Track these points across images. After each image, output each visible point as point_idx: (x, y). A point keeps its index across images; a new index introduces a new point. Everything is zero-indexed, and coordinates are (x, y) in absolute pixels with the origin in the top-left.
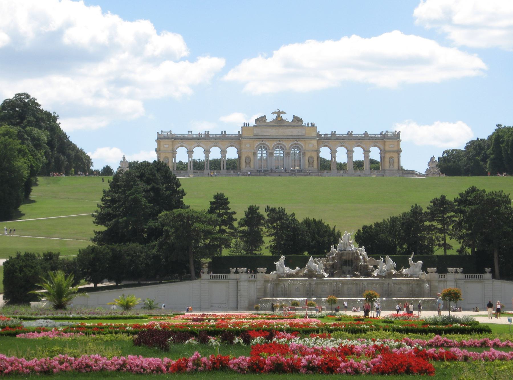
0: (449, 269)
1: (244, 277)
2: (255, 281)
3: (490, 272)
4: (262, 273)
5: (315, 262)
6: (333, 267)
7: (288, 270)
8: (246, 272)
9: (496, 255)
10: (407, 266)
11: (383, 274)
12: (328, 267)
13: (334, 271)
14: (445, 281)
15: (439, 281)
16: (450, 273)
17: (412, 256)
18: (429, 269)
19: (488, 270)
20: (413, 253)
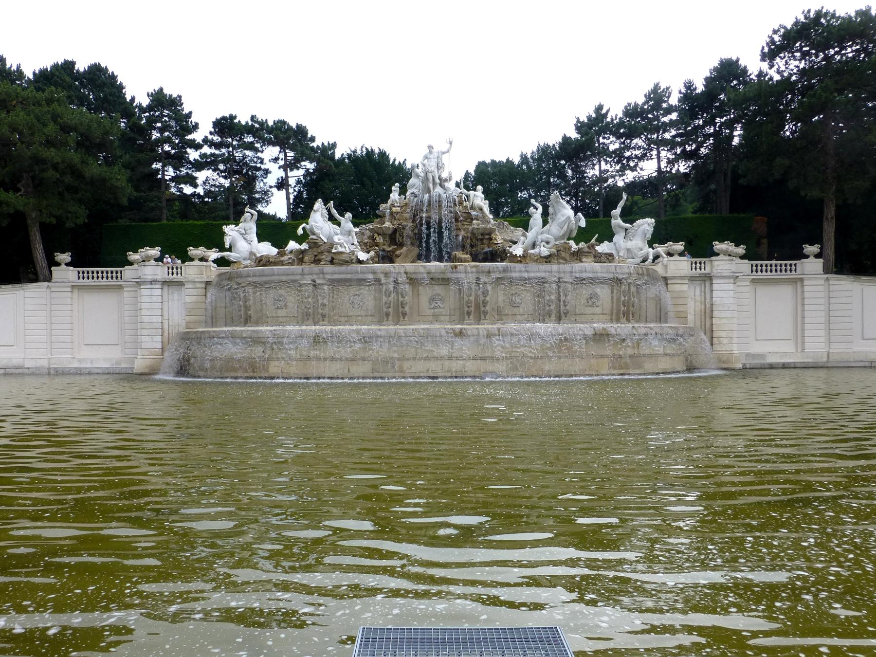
0: (718, 246)
1: (155, 271)
2: (181, 284)
3: (818, 256)
4: (202, 259)
5: (331, 218)
6: (394, 237)
7: (267, 249)
8: (160, 259)
9: (830, 211)
10: (609, 236)
11: (544, 251)
12: (379, 239)
13: (396, 250)
14: (708, 278)
15: (692, 279)
16: (721, 257)
17: (621, 204)
19: (811, 249)
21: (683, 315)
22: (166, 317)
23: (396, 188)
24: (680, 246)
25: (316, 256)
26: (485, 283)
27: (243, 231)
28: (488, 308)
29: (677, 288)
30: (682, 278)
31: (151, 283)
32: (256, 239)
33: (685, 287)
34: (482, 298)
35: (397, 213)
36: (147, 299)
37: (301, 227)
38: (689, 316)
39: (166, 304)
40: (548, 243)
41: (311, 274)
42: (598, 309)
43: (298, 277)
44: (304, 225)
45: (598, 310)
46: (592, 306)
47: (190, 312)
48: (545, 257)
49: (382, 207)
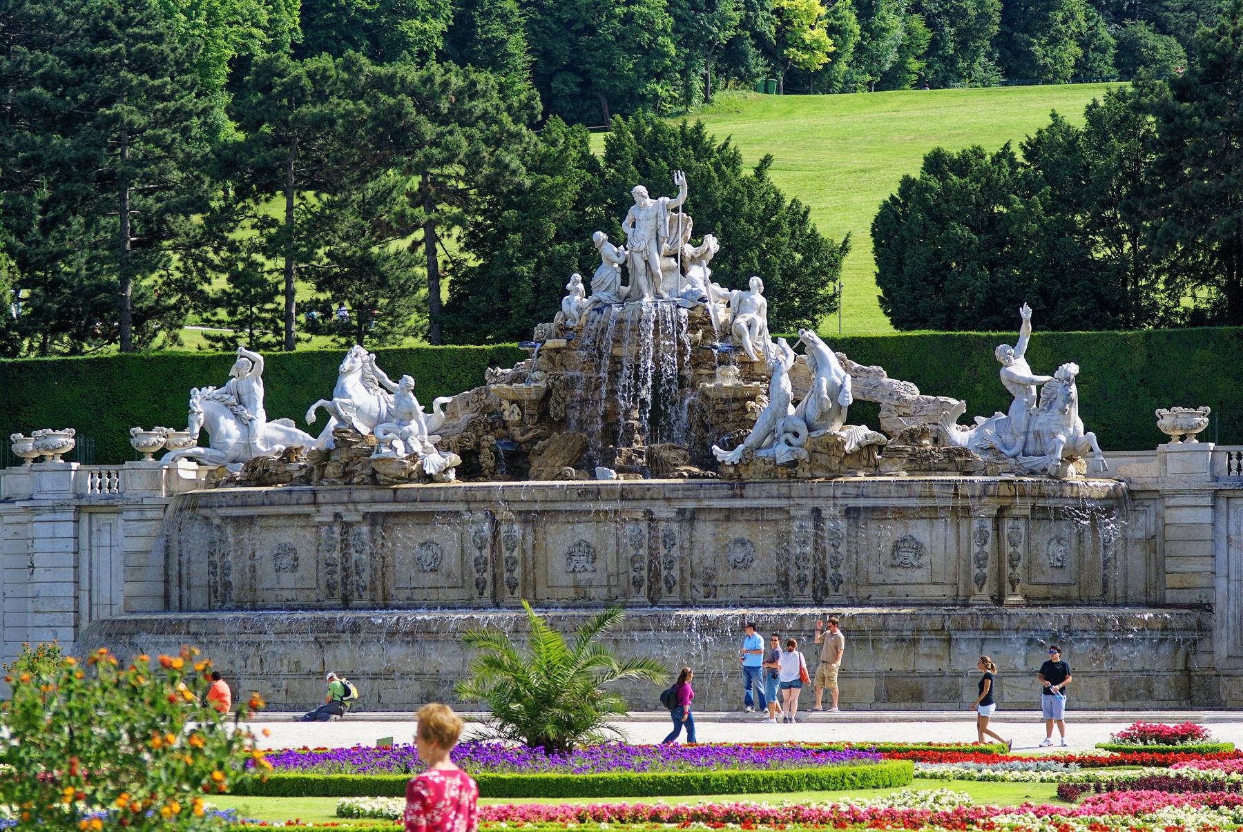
11: (782, 453)
18: (1167, 419)
20: (1026, 312)
21: (1202, 581)
22: (85, 585)
23: (576, 282)
24: (1200, 418)
25: (347, 464)
26: (668, 520)
27: (233, 400)
28: (675, 573)
29: (1186, 516)
30: (1196, 493)
31: (53, 510)
32: (261, 413)
33: (1206, 516)
34: (663, 551)
35: (558, 350)
36: (48, 546)
37: (314, 407)
38: (1221, 583)
39: (84, 556)
40: (796, 435)
41: (333, 504)
42: (918, 572)
43: (307, 509)
44: (321, 402)
45: (920, 575)
46: (903, 565)
47: (133, 572)
48: (783, 465)
49: (539, 330)
